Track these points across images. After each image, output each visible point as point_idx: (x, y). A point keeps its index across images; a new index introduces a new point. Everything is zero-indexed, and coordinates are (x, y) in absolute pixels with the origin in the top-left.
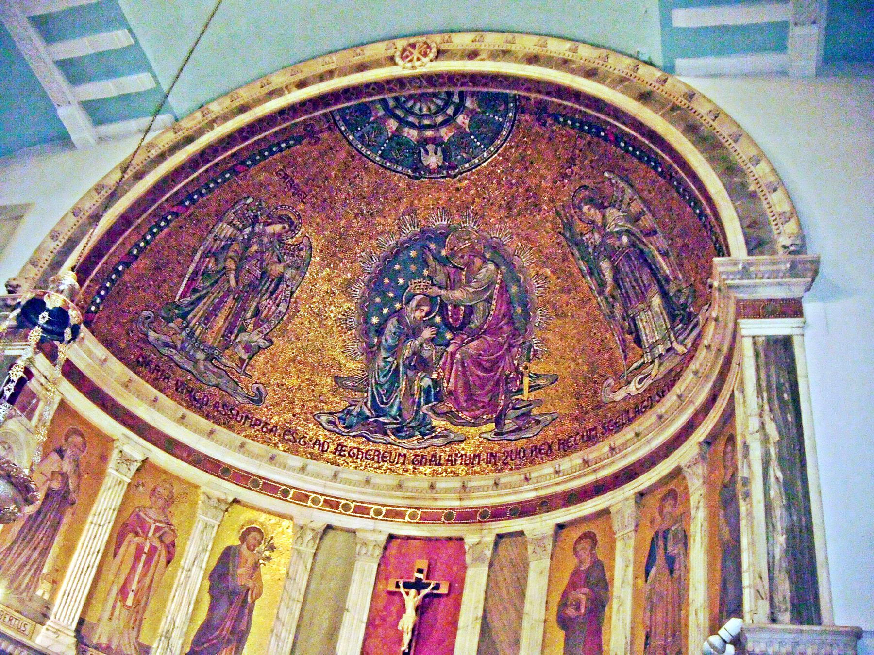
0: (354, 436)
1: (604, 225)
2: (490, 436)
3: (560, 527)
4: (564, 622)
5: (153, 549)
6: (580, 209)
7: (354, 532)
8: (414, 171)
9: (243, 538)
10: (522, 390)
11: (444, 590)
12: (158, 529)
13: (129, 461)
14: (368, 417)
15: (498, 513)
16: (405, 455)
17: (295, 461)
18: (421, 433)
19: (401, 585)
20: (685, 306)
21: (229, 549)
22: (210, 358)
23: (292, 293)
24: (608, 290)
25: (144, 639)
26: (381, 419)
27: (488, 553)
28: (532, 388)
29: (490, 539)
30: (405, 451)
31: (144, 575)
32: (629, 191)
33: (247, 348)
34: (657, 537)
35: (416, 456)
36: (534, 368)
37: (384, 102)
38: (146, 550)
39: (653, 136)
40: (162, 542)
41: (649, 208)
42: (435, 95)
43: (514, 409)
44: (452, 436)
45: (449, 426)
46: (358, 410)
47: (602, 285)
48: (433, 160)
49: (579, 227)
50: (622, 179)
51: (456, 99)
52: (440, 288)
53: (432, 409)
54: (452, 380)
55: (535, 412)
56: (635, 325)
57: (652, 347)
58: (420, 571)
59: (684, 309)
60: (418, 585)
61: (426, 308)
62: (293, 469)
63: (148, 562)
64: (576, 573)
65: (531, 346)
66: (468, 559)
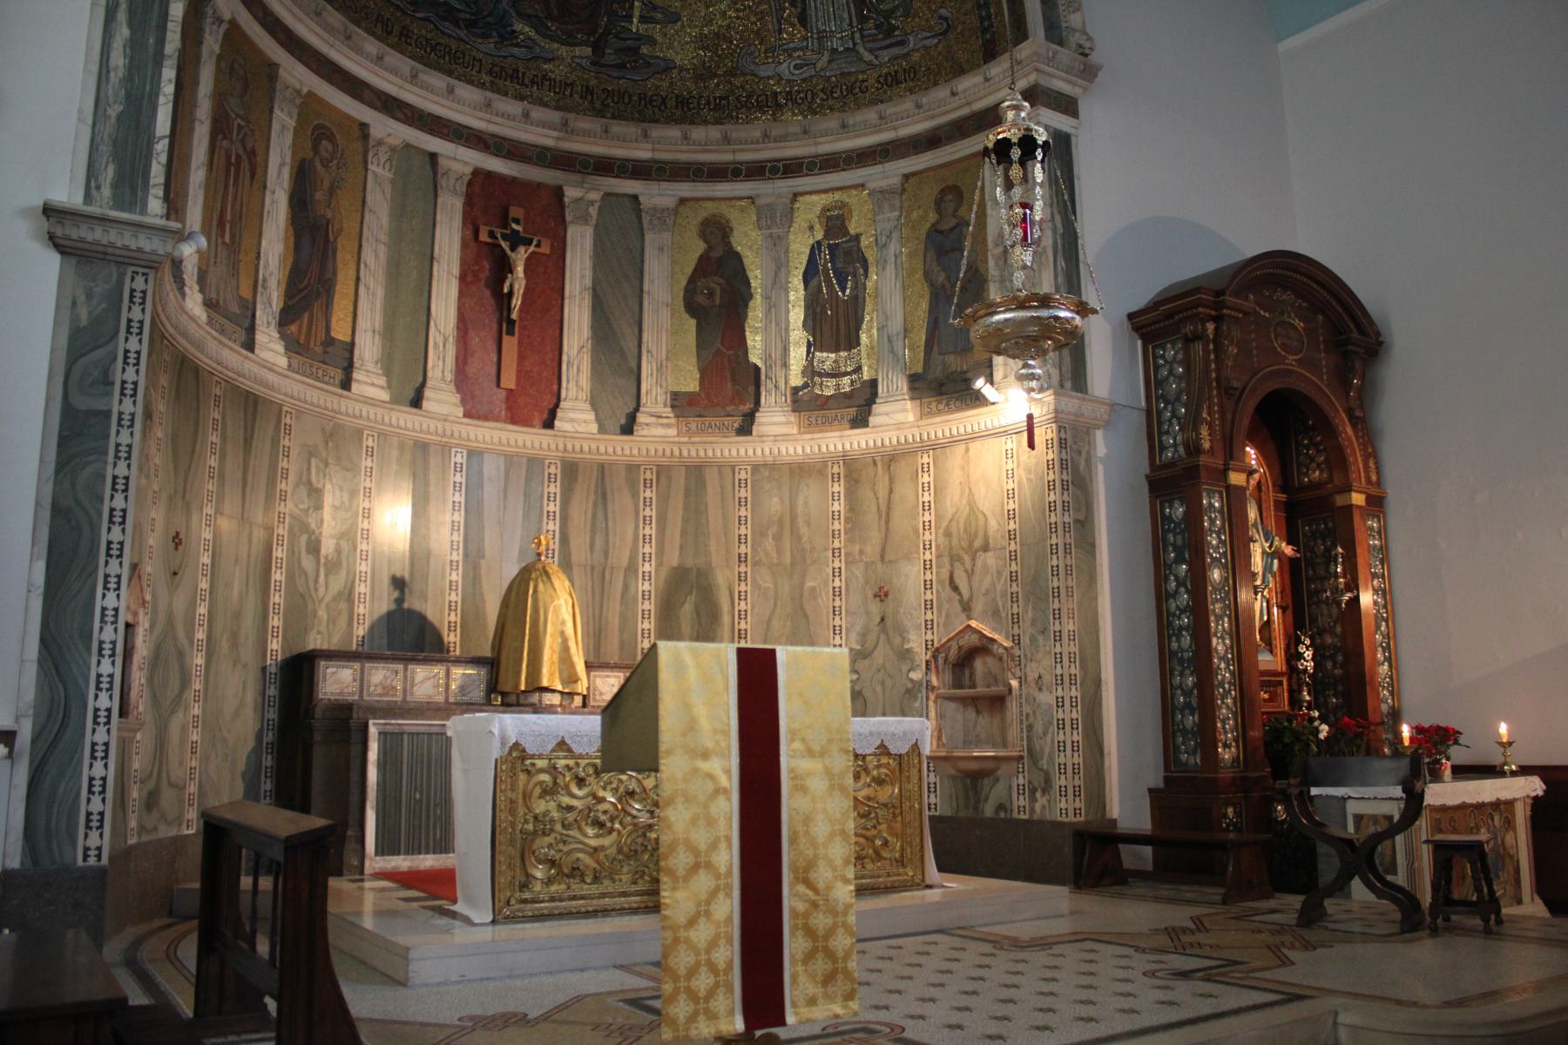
0: (420, 19)
3: (683, 201)
4: (691, 308)
5: (238, 156)
7: (433, 157)
9: (315, 149)
10: (631, 17)
11: (545, 249)
15: (605, 166)
16: (480, 60)
17: (372, 46)
18: (500, 36)
19: (499, 236)
20: (888, 15)
21: (303, 160)
25: (246, 292)
27: (593, 211)
28: (643, 19)
29: (595, 196)
31: (235, 198)
34: (819, 249)
35: (494, 65)
38: (233, 160)
40: (245, 149)
43: (616, 36)
45: (532, 34)
55: (645, 50)
57: (822, 37)
58: (517, 221)
59: (887, 18)
60: (516, 241)
62: (368, 57)
64: (703, 259)
66: (569, 217)
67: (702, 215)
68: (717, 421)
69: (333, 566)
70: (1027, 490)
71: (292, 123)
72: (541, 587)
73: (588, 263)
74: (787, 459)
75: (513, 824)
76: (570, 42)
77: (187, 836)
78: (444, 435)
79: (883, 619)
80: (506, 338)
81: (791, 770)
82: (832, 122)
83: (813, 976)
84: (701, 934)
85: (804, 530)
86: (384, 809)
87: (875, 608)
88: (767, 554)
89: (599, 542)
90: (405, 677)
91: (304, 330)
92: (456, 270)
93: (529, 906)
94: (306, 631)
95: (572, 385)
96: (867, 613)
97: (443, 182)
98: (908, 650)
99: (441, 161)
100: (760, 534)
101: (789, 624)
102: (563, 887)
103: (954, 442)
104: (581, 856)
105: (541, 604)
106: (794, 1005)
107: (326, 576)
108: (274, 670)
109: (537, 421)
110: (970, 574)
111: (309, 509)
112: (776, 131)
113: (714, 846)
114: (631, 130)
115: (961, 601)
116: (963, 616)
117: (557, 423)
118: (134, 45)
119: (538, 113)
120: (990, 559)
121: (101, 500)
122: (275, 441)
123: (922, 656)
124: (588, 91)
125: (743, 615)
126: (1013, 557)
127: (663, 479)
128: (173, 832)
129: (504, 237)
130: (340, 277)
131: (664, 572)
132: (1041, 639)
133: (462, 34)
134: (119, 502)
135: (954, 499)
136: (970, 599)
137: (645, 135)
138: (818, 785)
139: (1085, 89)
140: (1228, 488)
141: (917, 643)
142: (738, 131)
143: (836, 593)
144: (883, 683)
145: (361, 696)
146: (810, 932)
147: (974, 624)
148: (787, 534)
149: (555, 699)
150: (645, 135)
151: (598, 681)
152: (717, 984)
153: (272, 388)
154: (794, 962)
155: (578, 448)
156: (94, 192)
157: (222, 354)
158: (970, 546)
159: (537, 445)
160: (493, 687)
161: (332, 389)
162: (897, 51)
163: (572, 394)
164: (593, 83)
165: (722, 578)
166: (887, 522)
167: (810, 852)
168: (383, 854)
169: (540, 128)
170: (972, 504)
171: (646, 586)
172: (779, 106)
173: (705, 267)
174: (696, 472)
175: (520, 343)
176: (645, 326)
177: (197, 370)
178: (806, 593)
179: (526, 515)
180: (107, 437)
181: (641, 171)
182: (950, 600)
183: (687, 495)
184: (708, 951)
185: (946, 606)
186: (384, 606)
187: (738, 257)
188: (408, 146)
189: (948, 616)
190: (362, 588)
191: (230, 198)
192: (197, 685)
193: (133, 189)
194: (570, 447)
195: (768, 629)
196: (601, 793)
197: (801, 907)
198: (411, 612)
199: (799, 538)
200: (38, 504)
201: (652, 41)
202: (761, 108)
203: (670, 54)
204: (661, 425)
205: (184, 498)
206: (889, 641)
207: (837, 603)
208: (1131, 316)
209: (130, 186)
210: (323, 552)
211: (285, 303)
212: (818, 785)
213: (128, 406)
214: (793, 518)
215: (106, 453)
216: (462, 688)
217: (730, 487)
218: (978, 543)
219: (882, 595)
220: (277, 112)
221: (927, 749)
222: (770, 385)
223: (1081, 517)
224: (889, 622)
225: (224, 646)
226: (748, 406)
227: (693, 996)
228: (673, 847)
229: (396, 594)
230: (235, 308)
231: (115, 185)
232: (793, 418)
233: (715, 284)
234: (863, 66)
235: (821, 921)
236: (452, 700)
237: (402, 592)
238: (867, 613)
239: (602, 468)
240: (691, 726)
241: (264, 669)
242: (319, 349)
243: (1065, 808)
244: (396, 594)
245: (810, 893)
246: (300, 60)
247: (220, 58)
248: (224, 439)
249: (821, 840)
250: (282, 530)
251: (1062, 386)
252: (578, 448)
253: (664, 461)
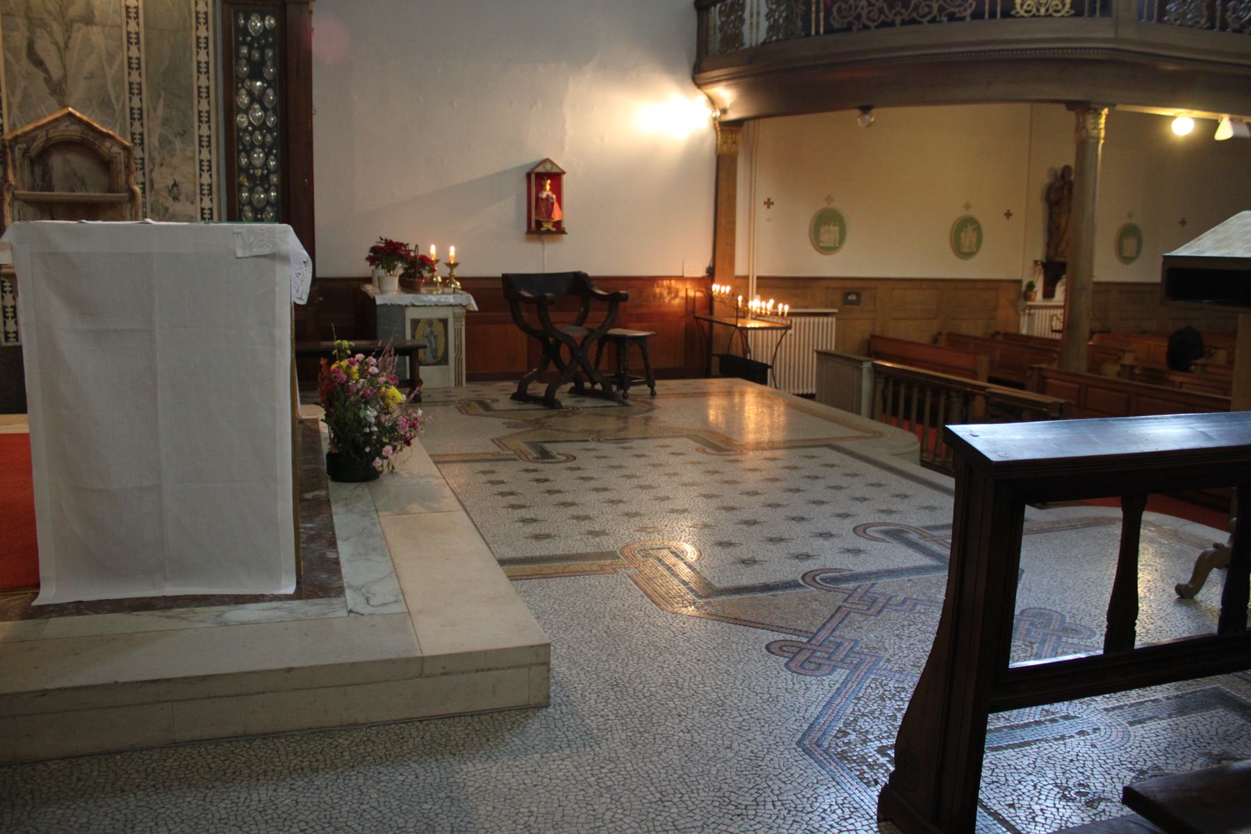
115: (48, 80)
116: (53, 101)
120: (97, 35)
132: (178, 144)
136: (65, 78)
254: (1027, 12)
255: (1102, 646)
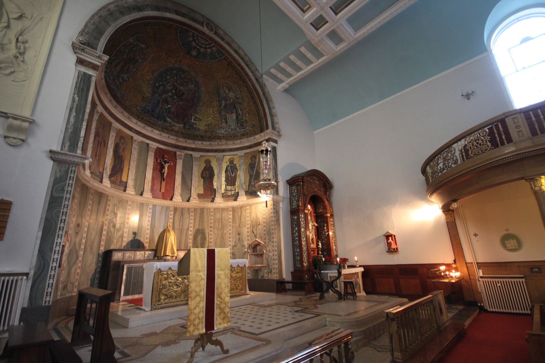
1: (228, 94)
2: (182, 128)
3: (201, 156)
4: (202, 177)
5: (101, 141)
6: (224, 87)
7: (148, 144)
8: (187, 52)
9: (120, 140)
11: (172, 164)
12: (102, 135)
13: (98, 113)
14: (150, 111)
15: (185, 148)
17: (135, 120)
20: (243, 123)
21: (117, 143)
22: (114, 80)
23: (138, 67)
24: (221, 108)
25: (101, 170)
26: (154, 113)
27: (183, 157)
28: (194, 120)
29: (183, 154)
30: (159, 124)
31: (100, 150)
32: (239, 92)
33: (123, 79)
35: (162, 126)
36: (196, 115)
37: (194, 33)
39: (256, 90)
40: (103, 139)
41: (242, 99)
42: (208, 41)
44: (172, 124)
45: (171, 121)
46: (147, 108)
47: (220, 106)
48: (194, 53)
49: (221, 91)
50: (239, 89)
51: (212, 45)
52: (178, 84)
53: (167, 115)
54: (174, 109)
55: (194, 126)
56: (226, 119)
57: (230, 126)
58: (166, 158)
60: (166, 162)
61: (172, 87)
62: (134, 122)
63: (100, 146)
65: (196, 109)
66: (177, 158)
67: (205, 159)
68: (207, 199)
69: (118, 230)
70: (267, 213)
71: (115, 135)
72: (168, 234)
73: (181, 167)
74: (221, 207)
75: (157, 287)
76: (178, 123)
77: (74, 295)
78: (147, 202)
79: (239, 239)
80: (162, 182)
81: (217, 274)
82: (231, 142)
83: (220, 318)
84: (197, 311)
85: (224, 221)
86: (126, 285)
87: (238, 237)
88: (216, 226)
89: (181, 223)
90: (134, 254)
91: (115, 179)
92: (152, 167)
93: (160, 306)
94: (110, 245)
95: (177, 192)
96: (236, 238)
97: (150, 149)
98: (244, 245)
99: (150, 145)
100: (215, 222)
101: (220, 240)
102: (168, 300)
103: (254, 204)
104: (173, 293)
105: (167, 237)
106: (216, 325)
107: (117, 232)
108: (101, 254)
109: (169, 198)
110: (256, 230)
111: (113, 218)
112: (220, 143)
113: (200, 291)
114: (191, 141)
116: (255, 238)
117: (173, 199)
118: (76, 117)
119: (171, 137)
120: (260, 227)
121: (59, 217)
122: (106, 202)
123: (247, 246)
124: (182, 133)
125: (211, 238)
126: (264, 226)
127: (195, 211)
128: (70, 295)
129: (163, 161)
130: (125, 168)
131: (195, 230)
132: (270, 243)
133: (155, 119)
134: (64, 217)
135: (253, 215)
137: (194, 143)
138: (223, 276)
139: (279, 139)
140: (305, 213)
141: (246, 244)
142: (213, 143)
143: (230, 234)
144: (239, 252)
145: (123, 259)
146: (220, 308)
147: (257, 240)
148: (220, 221)
149: (169, 258)
150: (194, 143)
151: (179, 253)
152: (200, 322)
153: (106, 192)
154: (216, 315)
155: (177, 204)
156: (63, 148)
157: (95, 184)
158: (256, 224)
159: (168, 204)
160: (155, 255)
161: (121, 192)
162: (244, 130)
163: (177, 193)
164: (183, 132)
165: (207, 231)
166: (240, 219)
167: (221, 291)
168: (125, 296)
169: (172, 140)
170: (257, 216)
171: (191, 233)
172: (221, 139)
173: (205, 169)
174: (202, 210)
175: (166, 183)
176: (193, 180)
177: (87, 187)
178: (224, 234)
179: (165, 218)
180: (62, 203)
181: (193, 149)
182: (252, 235)
183: (200, 214)
184: (198, 314)
185: (251, 236)
186: (131, 238)
187: (212, 167)
188: (142, 142)
189: (252, 238)
190: (125, 235)
191: (98, 150)
192: (80, 259)
193: (74, 148)
194: (176, 204)
195: (216, 241)
196: (178, 278)
197: (218, 303)
198: (137, 240)
199: (223, 223)
200: (41, 218)
201: (196, 124)
202: (217, 139)
203: (200, 127)
204: (195, 200)
205: (81, 216)
206: (240, 243)
207: (230, 236)
208: (287, 181)
209: (73, 146)
210: (116, 227)
211: (111, 173)
212: (223, 276)
213: (68, 196)
214: (222, 219)
215: (61, 206)
216: (148, 256)
217: (209, 213)
218: (258, 224)
219: (239, 234)
220: (111, 133)
221: (247, 266)
222: (218, 192)
223: (278, 219)
224: (240, 239)
225: (89, 249)
226: (213, 197)
227: (194, 325)
228: (192, 292)
229: (134, 236)
230: (98, 174)
231: (69, 147)
232: (222, 199)
233: (207, 172)
234: (237, 132)
235: (223, 306)
236: (145, 259)
237: (135, 235)
238: (236, 238)
239: (182, 208)
240: (197, 266)
241: (99, 254)
242: (119, 183)
243: (275, 276)
244: (134, 236)
245: (220, 300)
246: (117, 122)
247: (98, 120)
248: (93, 202)
249: (223, 288)
250: (106, 222)
251: (274, 194)
252: (177, 204)
253: (195, 207)
254: (474, 155)
255: (76, 305)
